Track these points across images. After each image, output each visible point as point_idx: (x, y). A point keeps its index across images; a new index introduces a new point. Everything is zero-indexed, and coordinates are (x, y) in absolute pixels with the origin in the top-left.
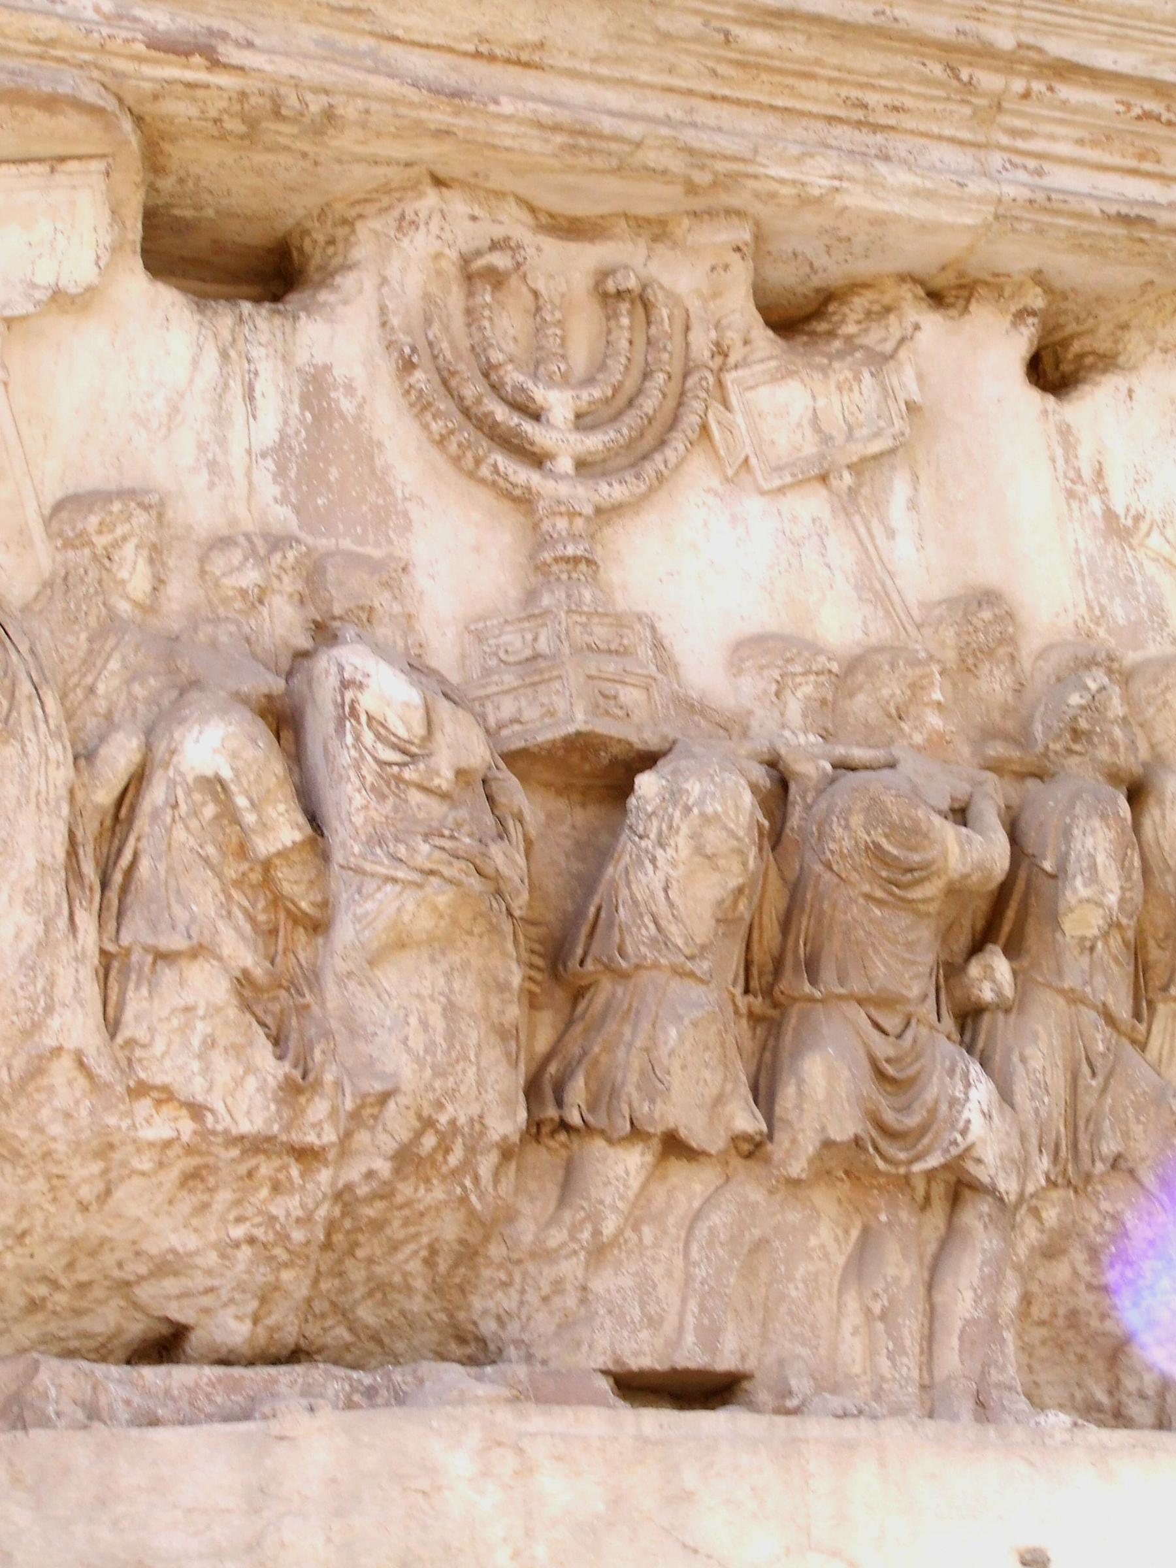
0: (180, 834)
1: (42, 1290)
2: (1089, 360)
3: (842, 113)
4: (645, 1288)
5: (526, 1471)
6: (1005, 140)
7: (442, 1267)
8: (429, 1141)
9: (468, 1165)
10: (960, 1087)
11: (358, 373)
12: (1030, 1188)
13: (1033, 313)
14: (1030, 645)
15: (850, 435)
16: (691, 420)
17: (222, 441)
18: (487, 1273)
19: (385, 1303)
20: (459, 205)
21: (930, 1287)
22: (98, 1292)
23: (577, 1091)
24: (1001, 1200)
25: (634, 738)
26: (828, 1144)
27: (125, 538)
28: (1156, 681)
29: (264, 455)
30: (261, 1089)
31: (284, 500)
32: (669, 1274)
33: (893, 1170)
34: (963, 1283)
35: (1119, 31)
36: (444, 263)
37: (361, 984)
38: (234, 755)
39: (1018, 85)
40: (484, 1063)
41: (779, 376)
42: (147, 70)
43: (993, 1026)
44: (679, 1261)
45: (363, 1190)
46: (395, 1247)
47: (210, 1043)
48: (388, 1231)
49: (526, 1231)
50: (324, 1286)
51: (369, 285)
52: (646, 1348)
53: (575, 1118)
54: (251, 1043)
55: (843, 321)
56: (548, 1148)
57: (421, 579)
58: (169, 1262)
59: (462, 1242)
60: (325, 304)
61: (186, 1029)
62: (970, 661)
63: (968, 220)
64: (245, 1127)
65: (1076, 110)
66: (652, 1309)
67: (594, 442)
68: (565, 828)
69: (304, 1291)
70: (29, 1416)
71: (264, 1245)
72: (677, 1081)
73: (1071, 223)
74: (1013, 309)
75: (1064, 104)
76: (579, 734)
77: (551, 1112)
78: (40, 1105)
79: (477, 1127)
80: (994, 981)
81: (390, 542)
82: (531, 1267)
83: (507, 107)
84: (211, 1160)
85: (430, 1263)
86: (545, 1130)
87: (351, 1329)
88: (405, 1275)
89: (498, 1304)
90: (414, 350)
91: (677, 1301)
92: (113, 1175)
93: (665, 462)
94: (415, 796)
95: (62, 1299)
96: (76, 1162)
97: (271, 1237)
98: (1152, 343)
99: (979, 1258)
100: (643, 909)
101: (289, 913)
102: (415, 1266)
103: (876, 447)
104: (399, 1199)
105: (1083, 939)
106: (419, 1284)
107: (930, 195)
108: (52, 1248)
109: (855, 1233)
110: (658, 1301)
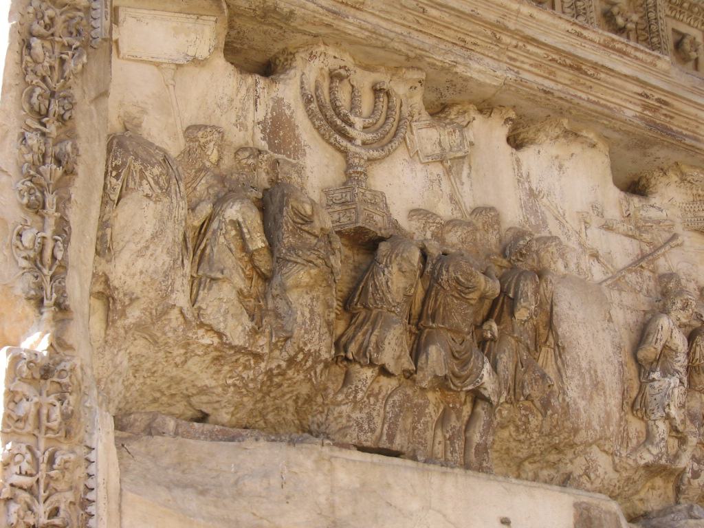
0: (222, 240)
1: (158, 395)
2: (526, 140)
3: (458, 43)
4: (370, 418)
5: (332, 470)
6: (508, 61)
7: (300, 404)
8: (301, 356)
9: (313, 367)
10: (480, 363)
11: (292, 102)
13: (511, 120)
14: (505, 226)
15: (451, 150)
17: (245, 117)
18: (315, 408)
19: (278, 414)
20: (331, 51)
21: (466, 431)
22: (178, 398)
23: (353, 348)
24: (491, 404)
25: (378, 232)
26: (436, 376)
28: (545, 243)
29: (259, 124)
30: (244, 330)
31: (264, 139)
32: (379, 415)
34: (477, 431)
36: (323, 72)
37: (281, 299)
38: (243, 213)
39: (514, 43)
41: (431, 126)
43: (490, 346)
44: (382, 411)
45: (275, 372)
46: (284, 395)
47: (227, 312)
48: (282, 388)
49: (331, 392)
51: (299, 74)
52: (369, 439)
53: (351, 357)
54: (242, 314)
55: (450, 114)
56: (339, 367)
57: (309, 174)
58: (205, 390)
59: (308, 395)
60: (282, 79)
61: (219, 308)
62: (486, 228)
63: (495, 84)
65: (531, 54)
66: (372, 426)
67: (369, 136)
68: (351, 261)
69: (250, 407)
70: (153, 432)
71: (239, 387)
72: (387, 347)
73: (528, 90)
74: (505, 117)
75: (528, 52)
76: (360, 227)
77: (343, 354)
78: (166, 325)
79: (317, 354)
80: (491, 330)
81: (299, 159)
82: (332, 407)
83: (351, 20)
84: (224, 354)
85: (296, 401)
86: (339, 360)
87: (265, 423)
88: (286, 404)
89: (318, 419)
90: (312, 97)
91: (380, 426)
93: (392, 147)
94: (307, 236)
95: (165, 399)
96: (176, 348)
97: (241, 385)
98: (547, 136)
99: (482, 423)
100: (378, 288)
101: (257, 273)
102: (290, 402)
103: (459, 154)
104: (288, 376)
105: (522, 320)
106: (291, 409)
107: (484, 73)
109: (441, 410)
110: (374, 423)
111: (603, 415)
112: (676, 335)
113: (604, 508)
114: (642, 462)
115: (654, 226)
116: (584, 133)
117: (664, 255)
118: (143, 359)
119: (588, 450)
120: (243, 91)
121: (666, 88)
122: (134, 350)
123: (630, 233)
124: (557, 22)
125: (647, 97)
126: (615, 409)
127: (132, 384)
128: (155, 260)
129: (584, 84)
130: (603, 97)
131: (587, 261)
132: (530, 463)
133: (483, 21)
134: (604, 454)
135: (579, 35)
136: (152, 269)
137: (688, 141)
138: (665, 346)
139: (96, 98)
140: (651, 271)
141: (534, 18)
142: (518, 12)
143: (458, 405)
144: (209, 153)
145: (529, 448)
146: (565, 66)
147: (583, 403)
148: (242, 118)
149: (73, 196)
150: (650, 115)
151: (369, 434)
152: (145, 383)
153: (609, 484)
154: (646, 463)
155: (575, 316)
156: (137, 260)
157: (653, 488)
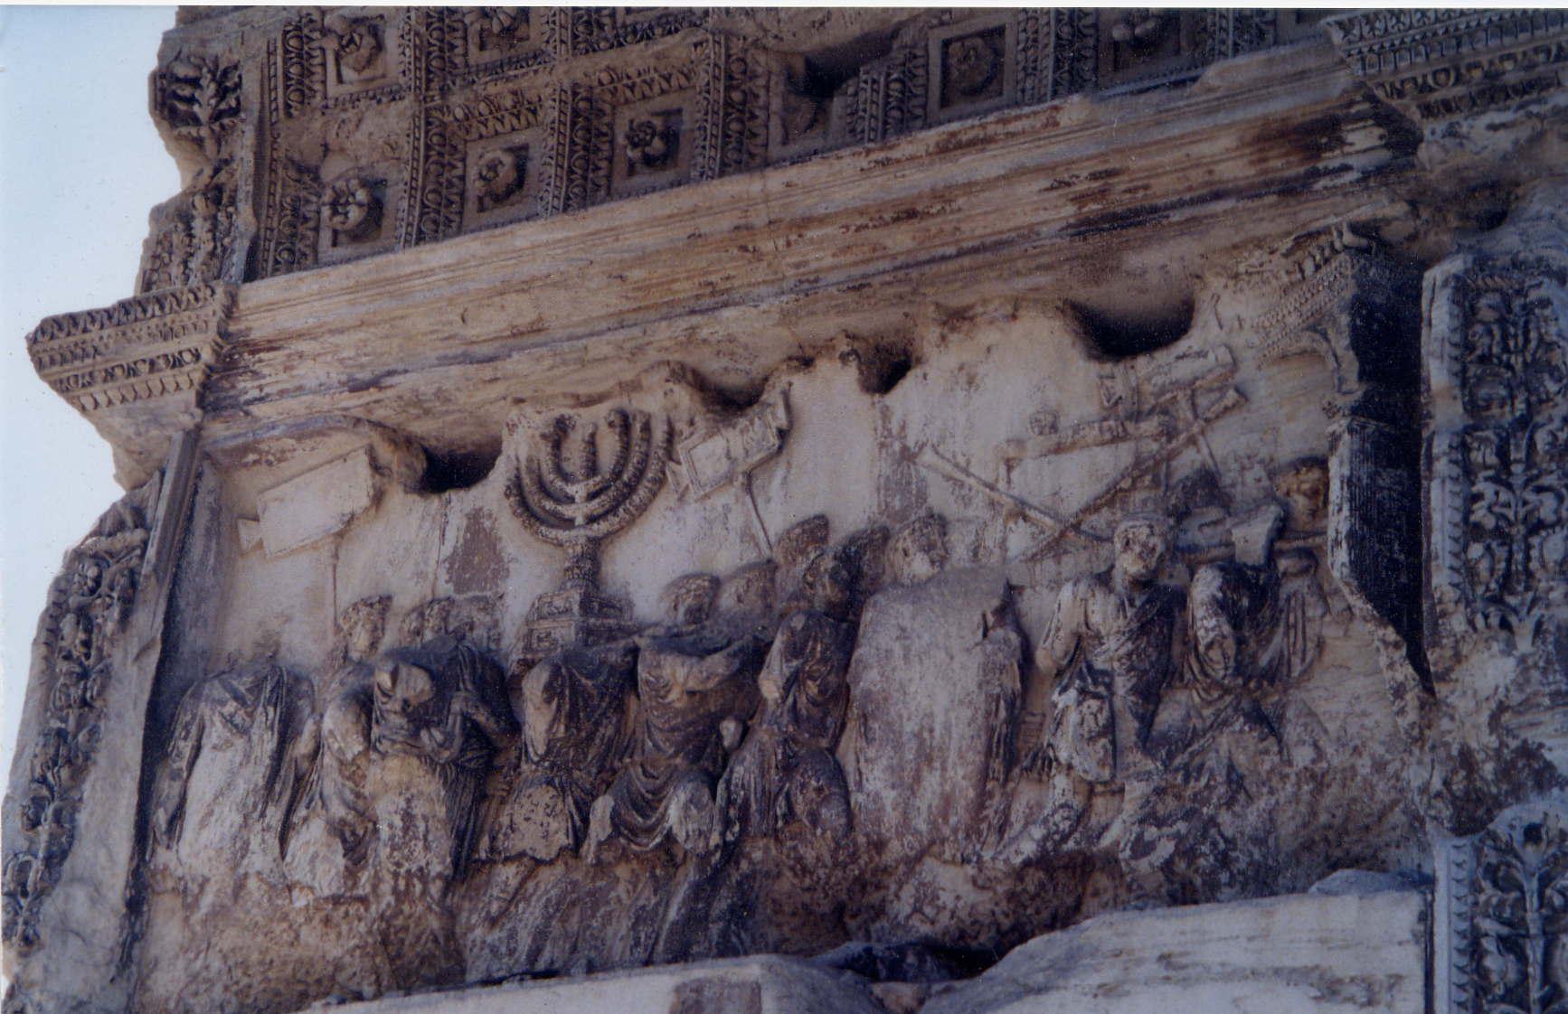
4: (512, 935)
8: (402, 884)
11: (495, 508)
17: (426, 563)
20: (528, 410)
39: (781, 242)
40: (430, 838)
41: (710, 435)
46: (418, 938)
50: (399, 962)
53: (483, 855)
57: (508, 600)
64: (327, 892)
67: (595, 506)
75: (812, 241)
85: (436, 940)
102: (430, 945)
103: (757, 457)
108: (290, 968)
112: (1096, 608)
113: (734, 979)
114: (1017, 860)
115: (1180, 395)
117: (1192, 441)
120: (427, 524)
121: (1093, 150)
123: (1108, 436)
124: (837, 165)
125: (1068, 184)
126: (964, 783)
127: (250, 986)
130: (988, 231)
131: (1000, 527)
132: (854, 916)
135: (885, 163)
138: (1079, 639)
139: (138, 658)
143: (658, 872)
146: (887, 224)
149: (85, 795)
151: (505, 960)
152: (268, 980)
155: (907, 650)
157: (1096, 894)
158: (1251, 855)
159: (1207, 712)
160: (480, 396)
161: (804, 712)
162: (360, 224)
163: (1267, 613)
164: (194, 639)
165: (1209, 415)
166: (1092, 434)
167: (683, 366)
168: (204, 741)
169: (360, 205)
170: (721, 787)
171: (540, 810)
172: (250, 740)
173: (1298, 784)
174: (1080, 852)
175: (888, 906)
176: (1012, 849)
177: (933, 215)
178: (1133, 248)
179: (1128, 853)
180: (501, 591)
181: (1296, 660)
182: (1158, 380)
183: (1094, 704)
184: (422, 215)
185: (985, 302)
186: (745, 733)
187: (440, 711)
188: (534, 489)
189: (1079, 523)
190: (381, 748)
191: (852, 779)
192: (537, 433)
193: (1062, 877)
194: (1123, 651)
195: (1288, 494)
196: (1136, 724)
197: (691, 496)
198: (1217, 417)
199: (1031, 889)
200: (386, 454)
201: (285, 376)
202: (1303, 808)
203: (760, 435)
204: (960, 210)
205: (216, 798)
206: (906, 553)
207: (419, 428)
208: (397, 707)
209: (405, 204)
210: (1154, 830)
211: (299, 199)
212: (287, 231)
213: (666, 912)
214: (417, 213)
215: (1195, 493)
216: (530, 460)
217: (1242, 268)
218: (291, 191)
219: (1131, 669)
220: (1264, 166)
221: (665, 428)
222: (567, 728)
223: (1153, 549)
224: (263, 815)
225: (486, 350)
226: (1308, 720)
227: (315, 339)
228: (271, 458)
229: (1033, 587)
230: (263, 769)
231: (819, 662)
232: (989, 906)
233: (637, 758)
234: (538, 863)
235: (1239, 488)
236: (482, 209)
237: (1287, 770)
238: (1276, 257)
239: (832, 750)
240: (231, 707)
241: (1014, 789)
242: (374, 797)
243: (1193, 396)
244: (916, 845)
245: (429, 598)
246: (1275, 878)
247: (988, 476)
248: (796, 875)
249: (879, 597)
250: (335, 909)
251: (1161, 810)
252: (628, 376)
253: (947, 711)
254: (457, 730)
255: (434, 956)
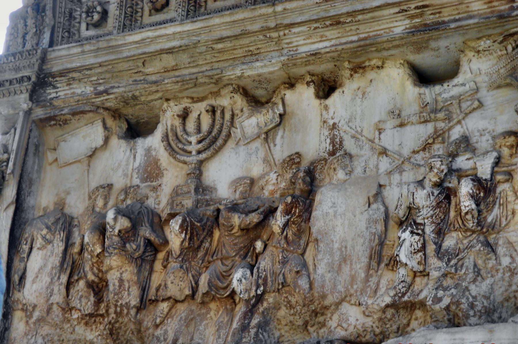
4: (166, 332)
6: (286, 46)
8: (118, 309)
11: (157, 146)
12: (252, 295)
13: (310, 82)
15: (266, 125)
16: (224, 133)
17: (127, 169)
20: (172, 103)
27: (98, 195)
30: (91, 304)
32: (171, 329)
33: (222, 297)
35: (301, 12)
40: (130, 290)
41: (250, 117)
42: (97, 100)
44: (174, 326)
45: (113, 321)
46: (125, 332)
47: (82, 297)
53: (153, 298)
57: (163, 187)
59: (136, 328)
63: (276, 68)
64: (87, 312)
65: (299, 33)
66: (166, 337)
67: (200, 146)
73: (300, 60)
75: (295, 33)
83: (166, 81)
85: (133, 333)
92: (73, 326)
96: (64, 325)
102: (130, 335)
103: (271, 126)
107: (265, 66)
111: (348, 278)
112: (417, 196)
114: (383, 305)
115: (454, 102)
116: (367, 64)
117: (459, 122)
118: (52, 336)
119: (340, 307)
122: (44, 333)
123: (422, 120)
125: (406, 11)
126: (360, 271)
128: (42, 282)
129: (351, 30)
130: (371, 30)
132: (312, 326)
133: (253, 32)
134: (354, 306)
136: (40, 288)
137: (453, 25)
138: (410, 208)
140: (440, 143)
141: (288, 9)
142: (274, 12)
144: (97, 203)
145: (300, 318)
146: (327, 27)
147: (329, 275)
148: (126, 171)
150: (419, 20)
153: (362, 327)
154: (386, 305)
155: (335, 212)
156: (32, 286)
157: (416, 319)
158: (483, 303)
159: (465, 242)
160: (150, 98)
161: (291, 238)
162: (98, 21)
163: (491, 199)
164: (30, 201)
165: (467, 112)
166: (414, 119)
167: (239, 87)
168: (33, 246)
169: (98, 13)
170: (255, 270)
171: (178, 278)
172: (53, 246)
173: (504, 274)
174: (410, 302)
175: (327, 323)
176: (382, 299)
177: (347, 23)
178: (434, 39)
179: (430, 302)
180: (160, 182)
181: (503, 220)
182: (445, 95)
183: (417, 238)
184: (125, 17)
185: (370, 60)
186: (266, 246)
187: (135, 235)
188: (174, 138)
189: (410, 158)
190: (109, 251)
191: (311, 268)
192: (175, 114)
193: (402, 312)
194: (429, 215)
195: (500, 147)
196: (434, 247)
197: (241, 143)
198: (470, 112)
199: (389, 317)
200: (110, 122)
201: (67, 88)
202: (506, 284)
203: (271, 117)
204: (359, 21)
205: (39, 270)
206: (335, 169)
207: (124, 111)
208: (116, 233)
209: (117, 12)
210: (441, 292)
211: (72, 9)
212: (67, 23)
213: (231, 324)
214: (123, 17)
215: (460, 146)
216: (172, 126)
217: (481, 49)
218: (69, 6)
219: (433, 222)
220: (490, 5)
221: (231, 113)
222: (189, 244)
223: (442, 171)
224: (59, 278)
225: (153, 78)
226: (508, 245)
227: (80, 72)
228: (61, 123)
229: (390, 186)
230: (59, 259)
231: (297, 217)
232: (371, 323)
233: (219, 256)
234: (177, 301)
235: (479, 143)
236: (150, 15)
237: (499, 267)
238: (496, 44)
239: (303, 254)
240: (45, 231)
241: (382, 273)
242: (107, 272)
243: (459, 103)
244: (339, 297)
245: (129, 185)
246: (493, 314)
247: (371, 137)
248: (287, 309)
249: (322, 189)
250: (90, 319)
251: (445, 284)
252: (215, 90)
253: (353, 240)
254: (142, 244)
255: (132, 340)
